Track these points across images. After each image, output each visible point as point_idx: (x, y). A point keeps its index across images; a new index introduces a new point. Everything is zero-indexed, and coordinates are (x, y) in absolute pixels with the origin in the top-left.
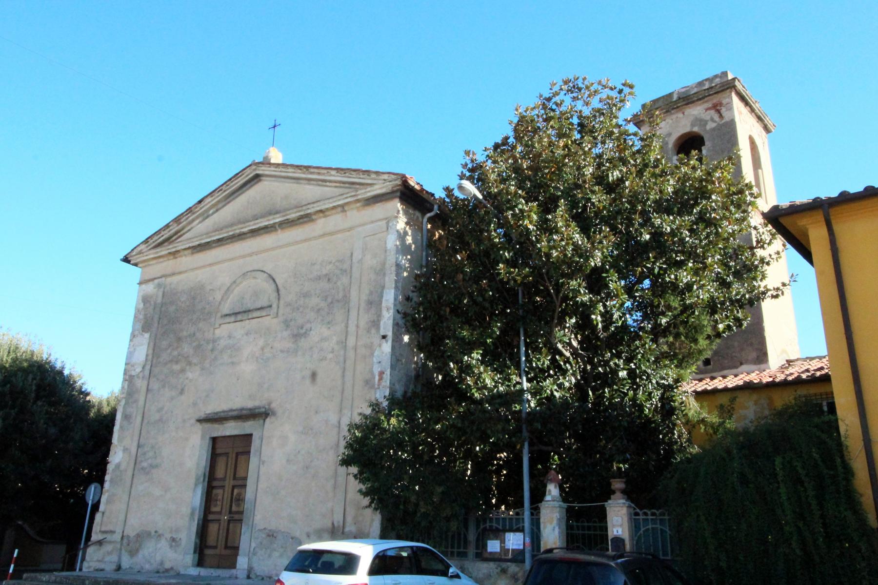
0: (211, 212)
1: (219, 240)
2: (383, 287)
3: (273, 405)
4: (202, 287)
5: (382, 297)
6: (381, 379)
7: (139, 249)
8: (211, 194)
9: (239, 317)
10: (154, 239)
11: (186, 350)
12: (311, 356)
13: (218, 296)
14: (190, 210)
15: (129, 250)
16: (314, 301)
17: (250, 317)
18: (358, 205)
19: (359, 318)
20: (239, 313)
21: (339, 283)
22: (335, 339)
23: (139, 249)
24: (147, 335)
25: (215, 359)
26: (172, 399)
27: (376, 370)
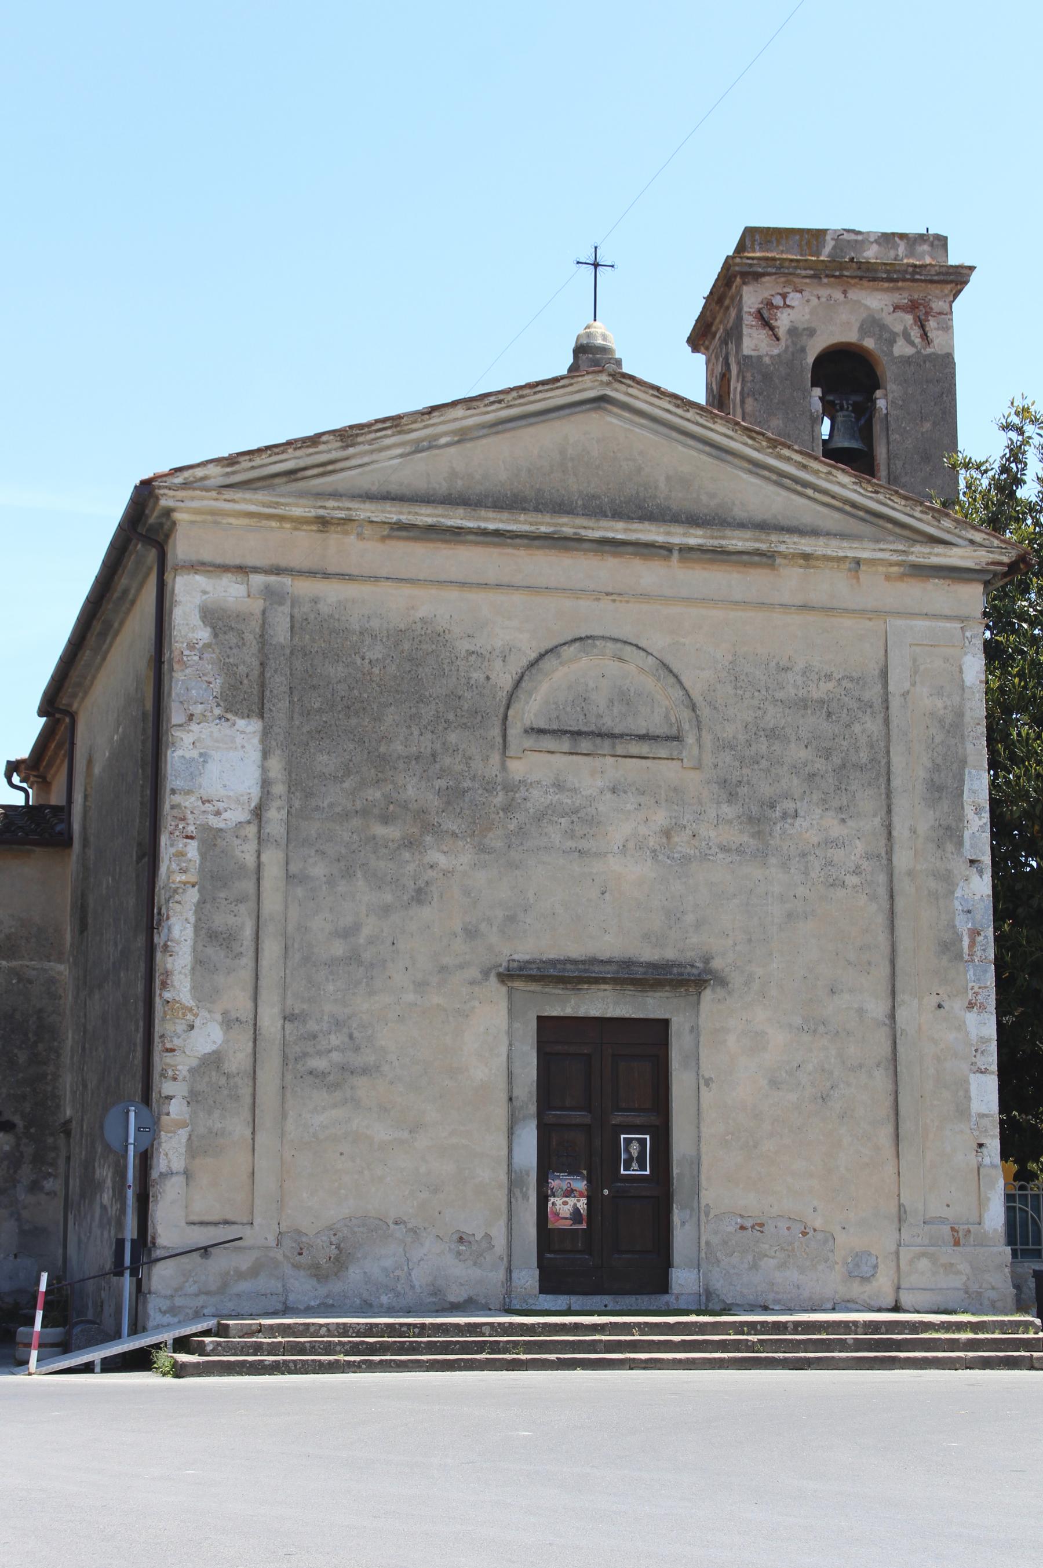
0: (443, 440)
1: (497, 533)
2: (963, 762)
3: (716, 964)
4: (439, 638)
5: (962, 781)
6: (973, 944)
7: (199, 473)
8: (468, 402)
9: (585, 745)
10: (258, 461)
11: (411, 792)
12: (806, 873)
13: (505, 680)
14: (395, 422)
15: (165, 469)
16: (798, 753)
17: (619, 751)
18: (895, 569)
19: (913, 817)
20: (579, 733)
21: (857, 728)
22: (860, 847)
23: (199, 473)
24: (249, 729)
25: (521, 831)
26: (386, 910)
27: (964, 926)
